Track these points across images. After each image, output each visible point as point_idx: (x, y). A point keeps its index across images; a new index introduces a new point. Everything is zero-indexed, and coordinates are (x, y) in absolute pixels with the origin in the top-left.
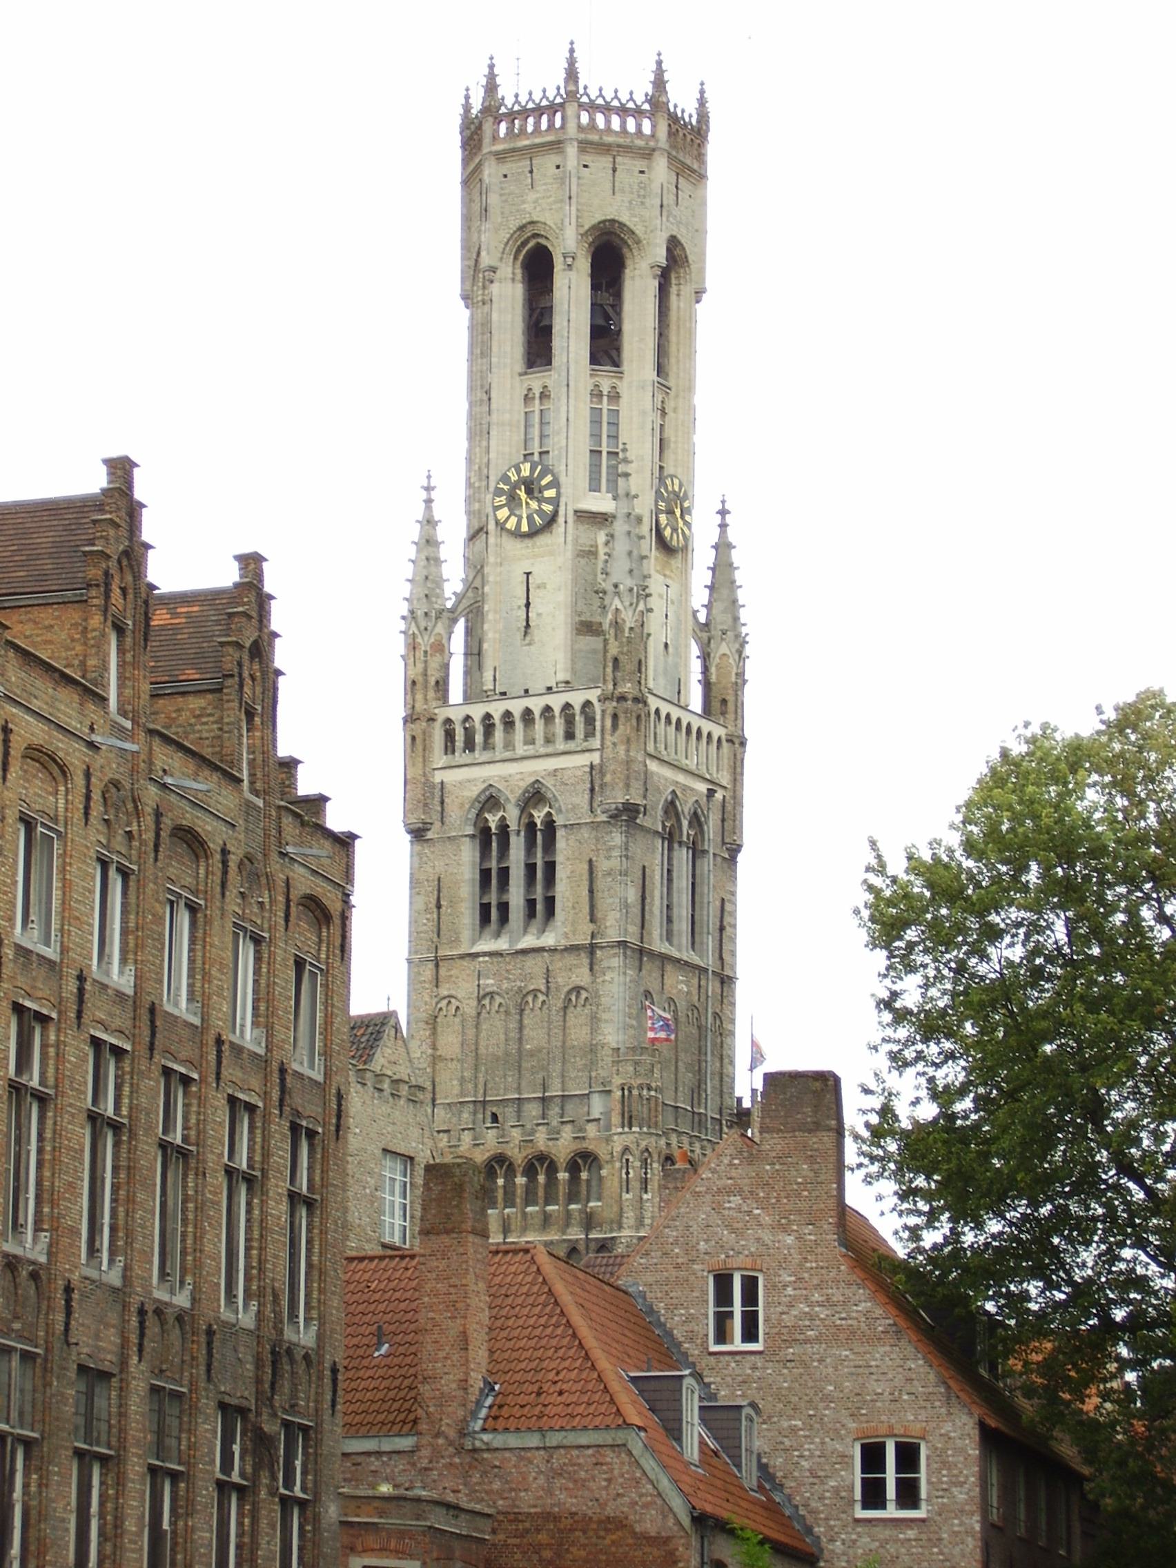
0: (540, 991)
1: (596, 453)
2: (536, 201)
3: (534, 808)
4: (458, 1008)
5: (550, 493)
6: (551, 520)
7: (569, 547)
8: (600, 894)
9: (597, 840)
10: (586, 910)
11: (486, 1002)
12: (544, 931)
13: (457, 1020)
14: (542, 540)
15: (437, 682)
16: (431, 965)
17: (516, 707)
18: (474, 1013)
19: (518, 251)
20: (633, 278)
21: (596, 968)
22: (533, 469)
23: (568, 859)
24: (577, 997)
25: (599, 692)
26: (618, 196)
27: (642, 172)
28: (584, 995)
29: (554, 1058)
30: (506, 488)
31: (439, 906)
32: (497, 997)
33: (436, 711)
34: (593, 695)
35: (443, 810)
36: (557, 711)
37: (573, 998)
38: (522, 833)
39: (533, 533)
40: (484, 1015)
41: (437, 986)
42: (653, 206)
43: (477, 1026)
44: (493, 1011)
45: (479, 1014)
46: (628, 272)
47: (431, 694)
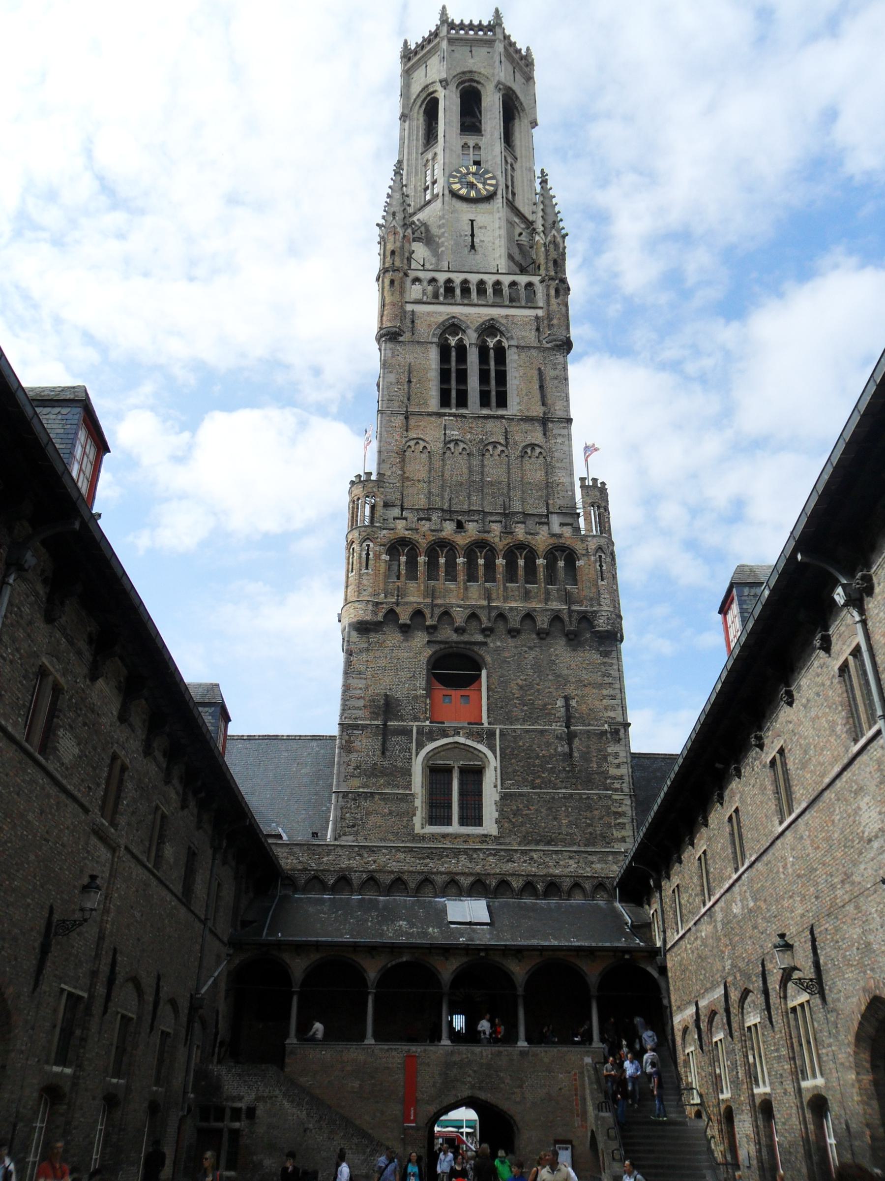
4: (425, 447)
8: (549, 390)
11: (452, 446)
13: (424, 456)
16: (402, 417)
18: (441, 451)
20: (520, 124)
24: (533, 449)
25: (539, 278)
28: (538, 450)
29: (515, 487)
30: (458, 175)
31: (409, 381)
32: (460, 443)
34: (536, 280)
35: (413, 327)
37: (529, 451)
40: (448, 453)
41: (407, 431)
44: (457, 453)
47: (405, 261)
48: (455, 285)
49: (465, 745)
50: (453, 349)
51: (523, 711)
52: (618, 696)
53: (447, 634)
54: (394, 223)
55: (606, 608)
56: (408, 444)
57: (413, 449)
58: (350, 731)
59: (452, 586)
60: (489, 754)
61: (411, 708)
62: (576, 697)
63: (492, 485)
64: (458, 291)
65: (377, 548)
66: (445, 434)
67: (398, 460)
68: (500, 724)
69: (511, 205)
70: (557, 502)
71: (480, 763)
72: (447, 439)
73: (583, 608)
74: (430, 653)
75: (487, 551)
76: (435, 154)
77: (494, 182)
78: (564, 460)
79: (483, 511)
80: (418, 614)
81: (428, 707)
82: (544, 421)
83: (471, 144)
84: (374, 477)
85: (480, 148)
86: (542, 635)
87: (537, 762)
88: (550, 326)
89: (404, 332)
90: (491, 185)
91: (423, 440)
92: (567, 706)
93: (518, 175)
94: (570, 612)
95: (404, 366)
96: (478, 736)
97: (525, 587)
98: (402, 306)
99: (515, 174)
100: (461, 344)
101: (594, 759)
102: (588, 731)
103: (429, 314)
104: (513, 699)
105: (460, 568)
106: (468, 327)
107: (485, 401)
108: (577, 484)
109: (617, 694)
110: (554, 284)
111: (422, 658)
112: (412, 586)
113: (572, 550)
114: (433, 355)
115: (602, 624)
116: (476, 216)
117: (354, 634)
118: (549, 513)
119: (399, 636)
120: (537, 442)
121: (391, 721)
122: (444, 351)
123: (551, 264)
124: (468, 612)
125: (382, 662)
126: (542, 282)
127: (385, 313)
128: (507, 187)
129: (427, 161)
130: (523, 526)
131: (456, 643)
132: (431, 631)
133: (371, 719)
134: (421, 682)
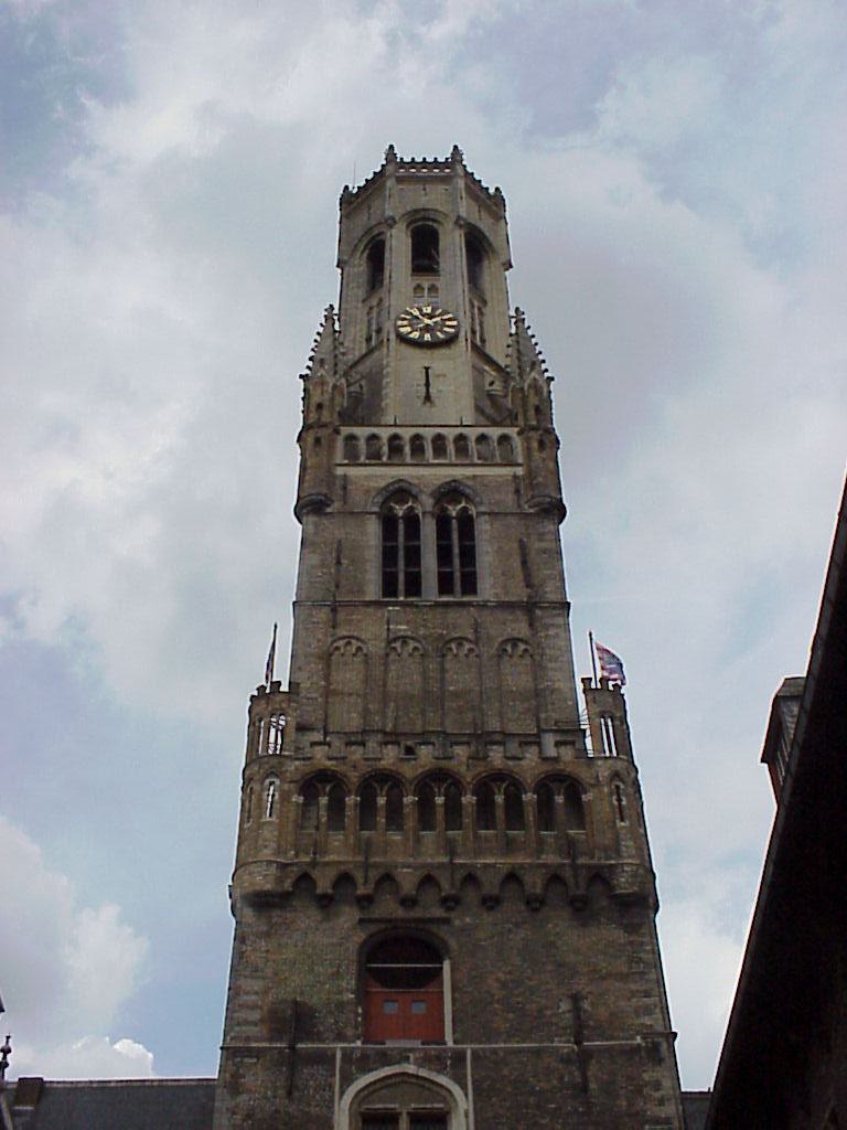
3: (449, 503)
4: (359, 649)
9: (527, 527)
10: (520, 575)
11: (398, 645)
18: (382, 652)
20: (490, 268)
24: (515, 646)
25: (516, 429)
28: (522, 647)
30: (408, 317)
31: (339, 563)
34: (512, 431)
35: (345, 494)
37: (509, 649)
40: (393, 656)
41: (334, 627)
44: (405, 654)
46: (486, 263)
48: (402, 443)
49: (417, 1077)
50: (401, 521)
51: (506, 1020)
52: (656, 992)
53: (388, 908)
54: (322, 372)
55: (630, 861)
56: (335, 645)
57: (342, 651)
58: (239, 1059)
59: (397, 837)
60: (456, 1090)
61: (332, 1021)
62: (590, 996)
64: (407, 449)
65: (286, 787)
66: (388, 629)
67: (320, 667)
68: (472, 1042)
69: (479, 351)
70: (552, 715)
71: (441, 1105)
72: (391, 635)
73: (595, 861)
74: (363, 936)
75: (450, 785)
76: (381, 300)
77: (455, 323)
78: (560, 659)
79: (444, 732)
80: (344, 879)
81: (360, 1019)
82: (530, 608)
83: (426, 285)
84: (284, 688)
85: (437, 289)
86: (535, 904)
87: (532, 1100)
88: (532, 486)
89: (333, 501)
91: (358, 639)
92: (577, 1010)
93: (488, 320)
94: (574, 867)
95: (332, 544)
96: (436, 1061)
97: (506, 835)
98: (330, 468)
99: (485, 319)
100: (412, 514)
101: (622, 1092)
102: (612, 1047)
103: (367, 477)
104: (491, 1003)
105: (406, 810)
106: (421, 491)
107: (445, 584)
108: (580, 687)
109: (652, 989)
110: (535, 435)
111: (350, 945)
112: (337, 840)
113: (576, 780)
114: (373, 528)
115: (624, 883)
117: (249, 913)
118: (541, 731)
119: (315, 913)
120: (521, 636)
121: (302, 1042)
122: (388, 522)
123: (532, 412)
124: (420, 873)
125: (289, 954)
126: (519, 434)
127: (307, 478)
128: (474, 332)
129: (371, 308)
130: (501, 749)
131: (402, 920)
132: (365, 904)
133: (270, 1040)
134: (349, 982)
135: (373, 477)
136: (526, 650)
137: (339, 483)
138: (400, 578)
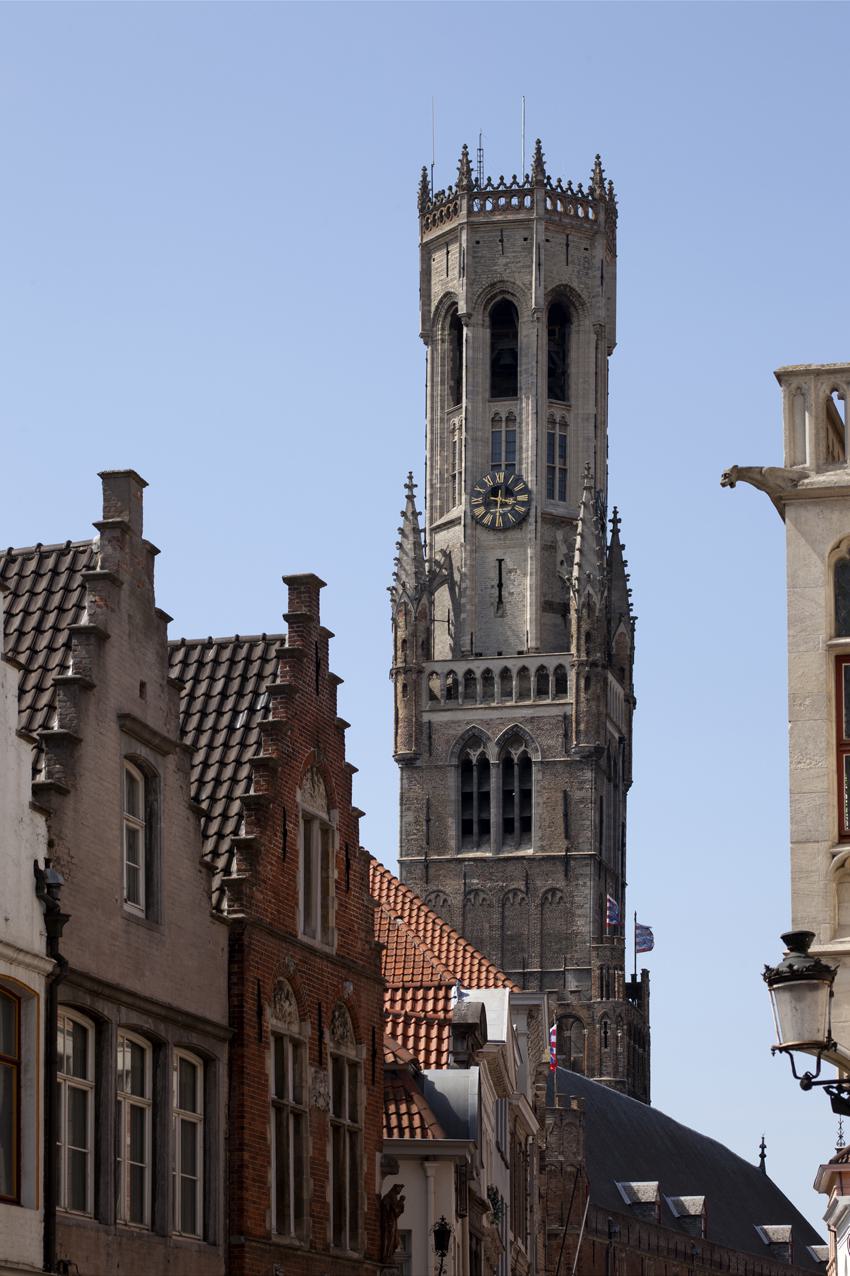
0: (520, 890)
1: (551, 470)
2: (506, 264)
4: (445, 901)
5: (523, 498)
6: (522, 520)
7: (538, 542)
8: (573, 817)
10: (561, 829)
11: (472, 896)
12: (520, 844)
14: (511, 534)
15: (423, 642)
16: (421, 866)
17: (496, 666)
18: (460, 905)
19: (488, 303)
20: (578, 332)
21: (570, 874)
22: (506, 478)
23: (545, 788)
26: (570, 265)
27: (586, 249)
28: (559, 895)
32: (481, 893)
33: (424, 665)
35: (431, 744)
36: (533, 671)
38: (501, 766)
39: (506, 528)
42: (594, 277)
43: (464, 915)
45: (464, 906)
46: (574, 327)
47: (420, 651)
50: (475, 768)
63: (512, 940)
90: (522, 504)
95: (423, 799)
103: (448, 724)
116: (505, 554)
122: (465, 767)
135: (454, 720)
136: (561, 898)
137: (425, 730)
138: (473, 830)
